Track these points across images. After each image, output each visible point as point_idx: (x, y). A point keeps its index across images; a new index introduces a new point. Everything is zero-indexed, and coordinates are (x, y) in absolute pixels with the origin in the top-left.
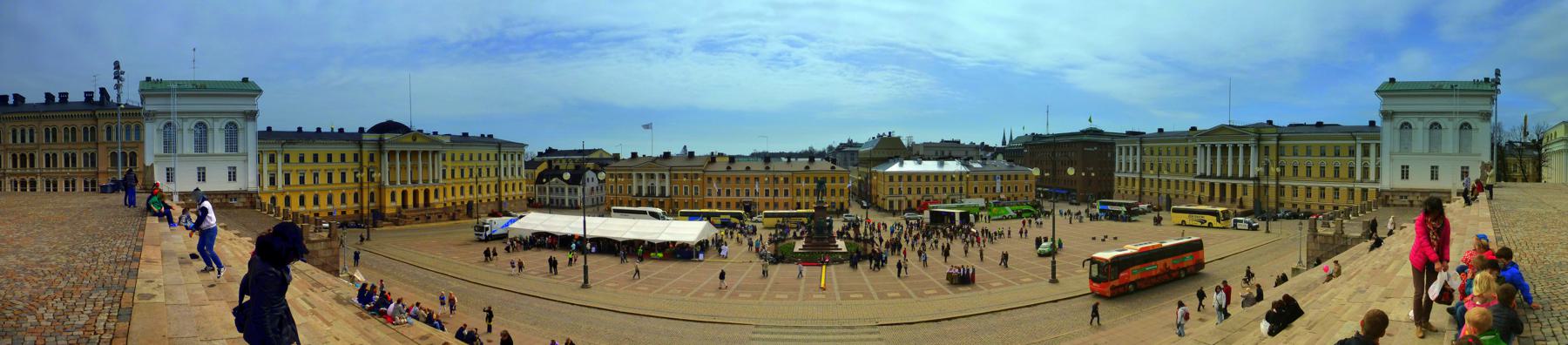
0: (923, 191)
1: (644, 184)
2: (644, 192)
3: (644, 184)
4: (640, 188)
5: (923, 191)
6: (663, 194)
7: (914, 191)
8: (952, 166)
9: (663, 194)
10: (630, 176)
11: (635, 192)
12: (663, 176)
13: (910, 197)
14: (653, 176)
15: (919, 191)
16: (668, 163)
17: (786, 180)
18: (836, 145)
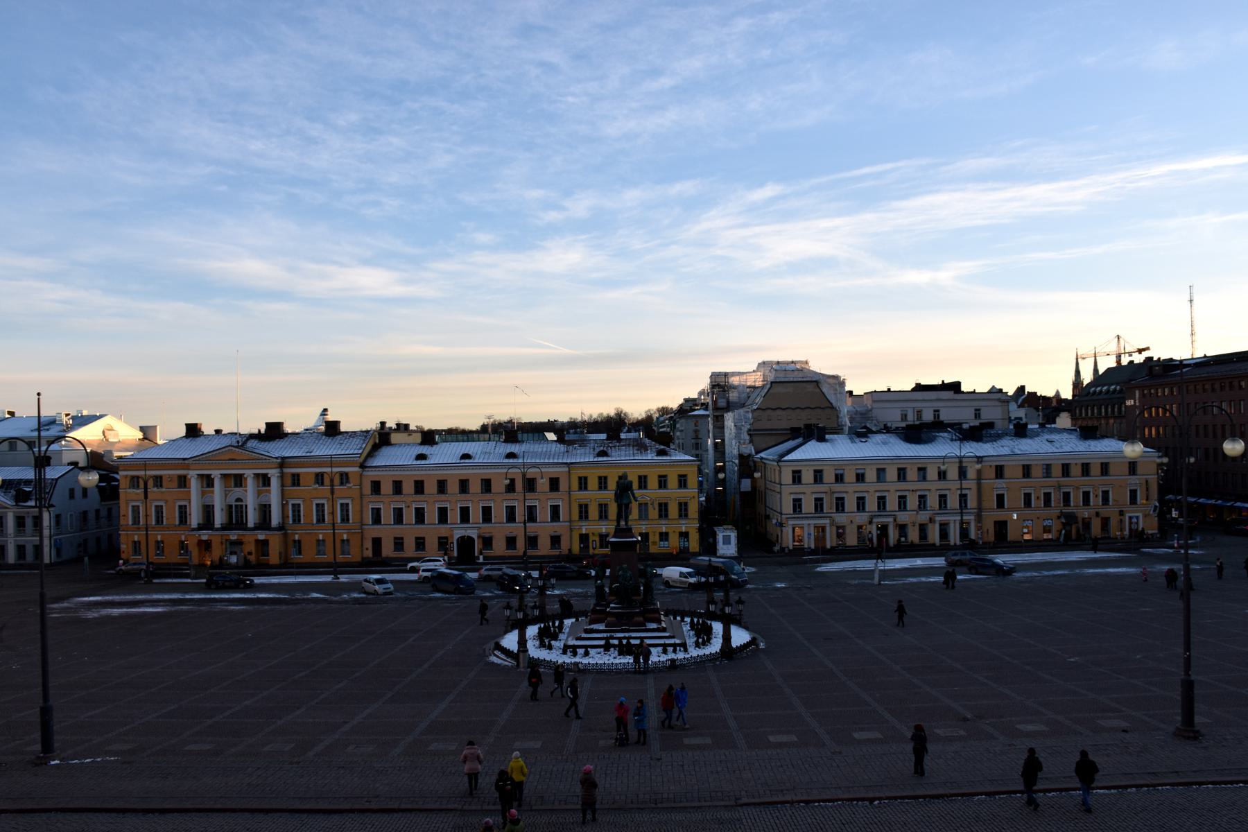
0: (872, 505)
1: (218, 498)
2: (219, 519)
3: (218, 498)
4: (208, 510)
5: (872, 505)
6: (264, 523)
7: (851, 504)
8: (942, 449)
9: (264, 523)
10: (183, 482)
11: (195, 519)
12: (265, 480)
13: (841, 518)
14: (239, 480)
15: (861, 504)
16: (277, 449)
17: (554, 484)
18: (674, 404)
